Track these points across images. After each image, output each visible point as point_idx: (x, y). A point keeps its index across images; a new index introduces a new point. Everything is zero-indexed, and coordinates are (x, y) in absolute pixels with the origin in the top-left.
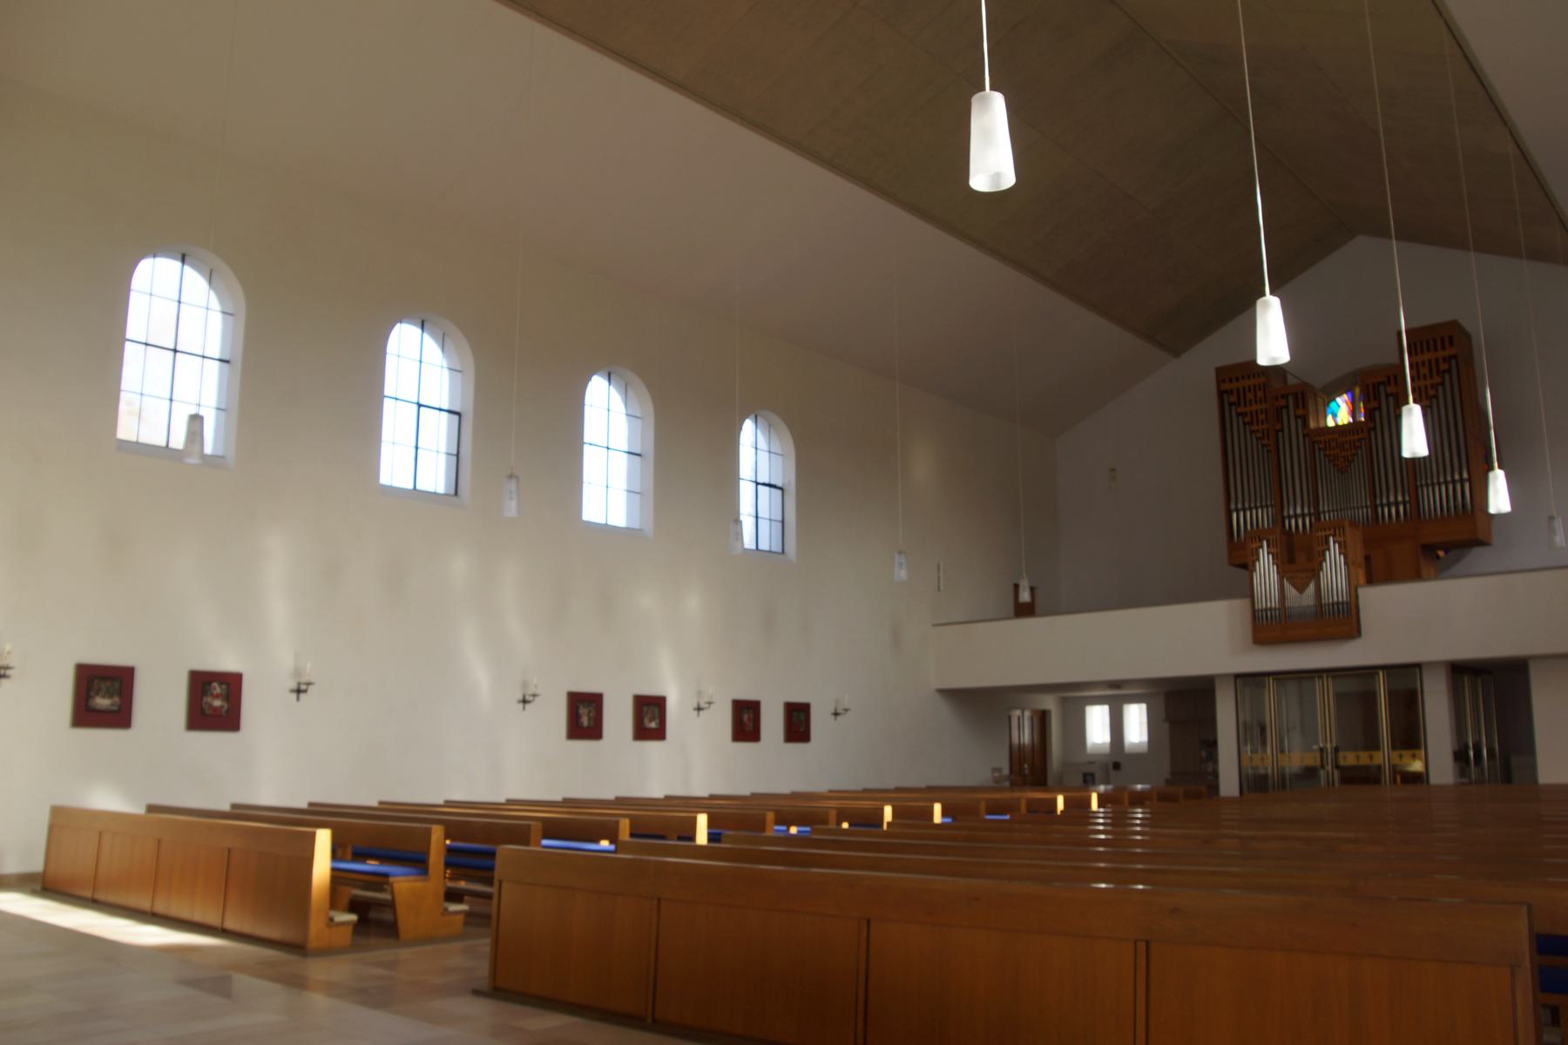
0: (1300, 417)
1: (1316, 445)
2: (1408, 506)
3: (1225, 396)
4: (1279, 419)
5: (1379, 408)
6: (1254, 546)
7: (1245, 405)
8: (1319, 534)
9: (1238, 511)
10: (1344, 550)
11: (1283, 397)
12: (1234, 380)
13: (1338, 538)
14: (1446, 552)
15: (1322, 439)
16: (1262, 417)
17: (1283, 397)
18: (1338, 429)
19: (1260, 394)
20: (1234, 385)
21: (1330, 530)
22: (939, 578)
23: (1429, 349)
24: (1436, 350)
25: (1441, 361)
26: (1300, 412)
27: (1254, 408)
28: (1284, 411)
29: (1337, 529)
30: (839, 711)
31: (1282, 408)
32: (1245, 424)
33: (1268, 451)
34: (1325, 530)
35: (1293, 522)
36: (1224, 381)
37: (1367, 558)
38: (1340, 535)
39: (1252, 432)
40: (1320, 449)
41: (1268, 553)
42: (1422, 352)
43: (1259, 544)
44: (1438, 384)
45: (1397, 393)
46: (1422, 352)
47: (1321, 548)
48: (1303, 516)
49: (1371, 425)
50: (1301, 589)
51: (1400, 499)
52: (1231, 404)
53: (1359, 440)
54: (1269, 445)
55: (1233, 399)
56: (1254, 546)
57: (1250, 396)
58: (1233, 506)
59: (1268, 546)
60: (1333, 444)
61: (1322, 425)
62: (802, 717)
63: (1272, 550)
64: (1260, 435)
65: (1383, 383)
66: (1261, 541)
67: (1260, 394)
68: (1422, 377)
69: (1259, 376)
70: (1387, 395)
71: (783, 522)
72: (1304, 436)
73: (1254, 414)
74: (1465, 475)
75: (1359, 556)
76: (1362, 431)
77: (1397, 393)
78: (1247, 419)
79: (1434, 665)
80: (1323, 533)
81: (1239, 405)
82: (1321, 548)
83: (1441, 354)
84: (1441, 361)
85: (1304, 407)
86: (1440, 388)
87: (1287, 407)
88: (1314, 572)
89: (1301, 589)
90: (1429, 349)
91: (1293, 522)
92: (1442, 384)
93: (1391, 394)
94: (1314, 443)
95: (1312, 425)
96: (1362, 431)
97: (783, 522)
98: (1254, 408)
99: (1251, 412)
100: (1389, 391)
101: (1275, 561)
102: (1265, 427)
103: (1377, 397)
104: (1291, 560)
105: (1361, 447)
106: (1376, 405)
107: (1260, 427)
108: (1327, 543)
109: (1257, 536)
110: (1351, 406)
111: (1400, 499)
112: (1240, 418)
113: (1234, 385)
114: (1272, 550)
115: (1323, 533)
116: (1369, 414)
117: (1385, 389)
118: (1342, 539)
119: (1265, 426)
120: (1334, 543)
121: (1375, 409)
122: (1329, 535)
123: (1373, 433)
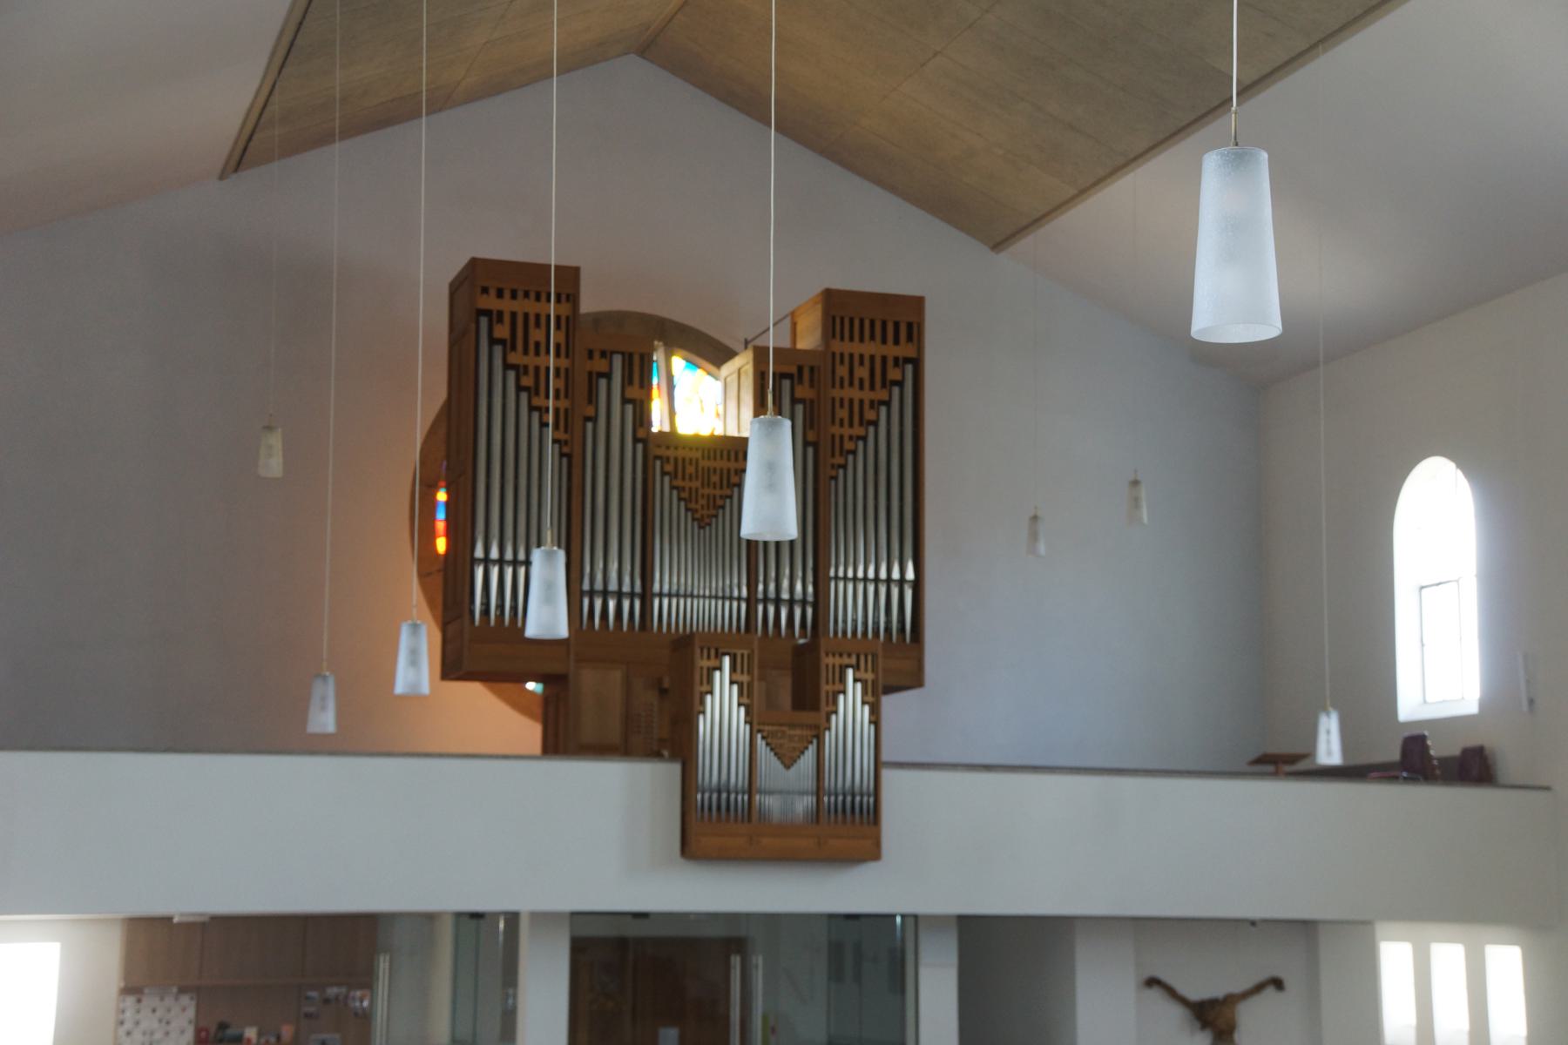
1: (658, 463)
2: (809, 611)
3: (484, 321)
4: (592, 397)
6: (705, 663)
7: (526, 352)
8: (830, 660)
9: (487, 561)
11: (603, 354)
12: (507, 294)
13: (862, 675)
15: (671, 453)
17: (603, 354)
20: (506, 305)
21: (849, 655)
23: (872, 337)
24: (884, 341)
25: (890, 363)
26: (634, 392)
28: (603, 382)
31: (601, 375)
34: (841, 655)
35: (598, 603)
36: (485, 290)
38: (866, 670)
40: (664, 473)
41: (732, 683)
42: (862, 340)
43: (713, 663)
45: (812, 401)
46: (862, 340)
47: (830, 688)
50: (788, 761)
52: (493, 341)
54: (566, 443)
56: (705, 663)
59: (733, 669)
63: (738, 677)
66: (719, 656)
68: (856, 382)
72: (636, 440)
74: (910, 575)
79: (937, 921)
80: (838, 661)
82: (830, 688)
83: (891, 351)
84: (890, 363)
85: (642, 386)
86: (883, 410)
87: (608, 376)
88: (818, 733)
89: (788, 761)
90: (872, 337)
91: (598, 603)
92: (888, 404)
94: (657, 457)
99: (537, 369)
100: (798, 395)
101: (745, 700)
108: (843, 680)
109: (717, 644)
111: (494, 554)
112: (511, 375)
113: (506, 305)
114: (738, 677)
120: (855, 680)
122: (848, 666)
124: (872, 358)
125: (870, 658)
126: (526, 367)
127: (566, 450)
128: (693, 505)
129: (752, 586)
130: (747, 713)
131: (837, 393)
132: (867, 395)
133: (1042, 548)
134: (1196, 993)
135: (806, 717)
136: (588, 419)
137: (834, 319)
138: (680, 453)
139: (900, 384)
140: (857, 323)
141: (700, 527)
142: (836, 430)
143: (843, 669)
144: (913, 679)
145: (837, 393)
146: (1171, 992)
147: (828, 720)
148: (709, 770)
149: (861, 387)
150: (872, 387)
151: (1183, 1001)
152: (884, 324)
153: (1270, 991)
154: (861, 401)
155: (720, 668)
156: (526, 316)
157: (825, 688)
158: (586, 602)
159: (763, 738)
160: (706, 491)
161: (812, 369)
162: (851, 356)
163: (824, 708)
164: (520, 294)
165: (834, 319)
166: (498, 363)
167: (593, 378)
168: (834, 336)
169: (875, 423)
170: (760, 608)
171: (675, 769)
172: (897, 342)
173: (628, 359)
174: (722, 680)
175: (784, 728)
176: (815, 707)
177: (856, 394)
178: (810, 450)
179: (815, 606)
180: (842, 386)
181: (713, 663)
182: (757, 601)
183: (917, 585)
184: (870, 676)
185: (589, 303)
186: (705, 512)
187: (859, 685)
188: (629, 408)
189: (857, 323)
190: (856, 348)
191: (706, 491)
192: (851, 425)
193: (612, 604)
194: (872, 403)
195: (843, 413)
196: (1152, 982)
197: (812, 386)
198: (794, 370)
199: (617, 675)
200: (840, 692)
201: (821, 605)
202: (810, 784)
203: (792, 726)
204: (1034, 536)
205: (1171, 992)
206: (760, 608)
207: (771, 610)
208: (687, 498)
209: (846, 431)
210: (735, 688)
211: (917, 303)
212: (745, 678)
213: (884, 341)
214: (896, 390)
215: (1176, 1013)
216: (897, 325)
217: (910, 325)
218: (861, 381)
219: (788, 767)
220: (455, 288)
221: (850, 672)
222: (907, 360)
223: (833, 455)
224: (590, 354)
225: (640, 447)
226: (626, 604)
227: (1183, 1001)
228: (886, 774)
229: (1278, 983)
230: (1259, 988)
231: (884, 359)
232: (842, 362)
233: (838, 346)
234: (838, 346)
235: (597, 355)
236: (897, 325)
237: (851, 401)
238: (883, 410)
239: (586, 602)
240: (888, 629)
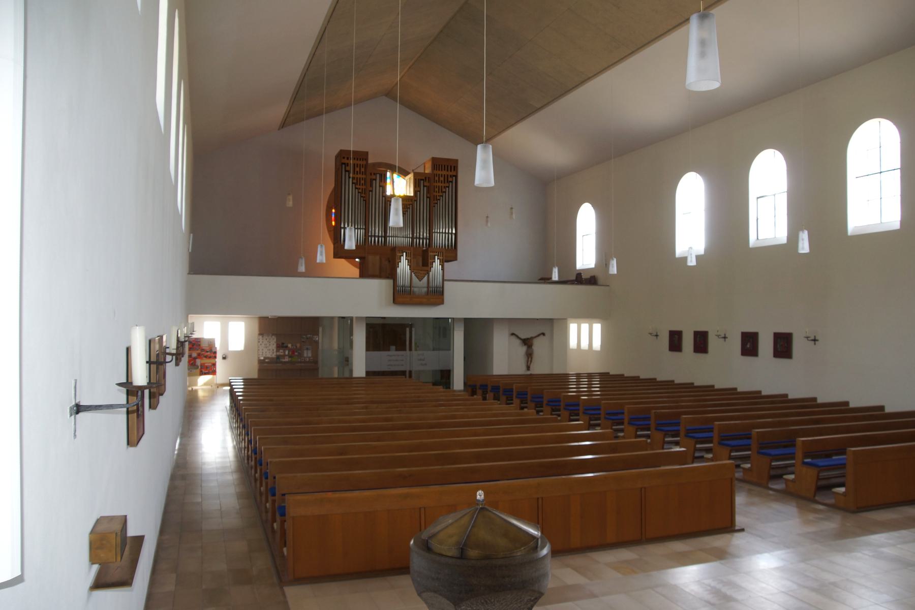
2: (428, 241)
3: (344, 166)
4: (371, 186)
5: (420, 191)
8: (431, 254)
11: (374, 174)
16: (362, 182)
17: (374, 174)
23: (445, 170)
24: (448, 171)
28: (374, 181)
31: (374, 179)
33: (363, 200)
35: (373, 239)
36: (344, 158)
41: (406, 259)
43: (401, 254)
44: (447, 187)
46: (442, 170)
47: (431, 261)
49: (416, 199)
50: (420, 279)
53: (409, 205)
54: (365, 197)
65: (423, 180)
66: (403, 252)
67: (363, 170)
69: (363, 160)
70: (424, 186)
72: (383, 196)
73: (359, 179)
74: (454, 232)
79: (459, 319)
80: (433, 254)
83: (450, 173)
86: (447, 189)
87: (376, 180)
88: (428, 272)
89: (420, 279)
90: (445, 170)
91: (373, 239)
92: (449, 187)
93: (426, 186)
99: (357, 178)
100: (425, 184)
102: (364, 187)
103: (419, 186)
106: (419, 190)
107: (361, 187)
108: (434, 259)
109: (402, 249)
115: (433, 254)
116: (415, 192)
117: (423, 183)
119: (364, 187)
121: (418, 191)
124: (444, 175)
127: (364, 199)
129: (413, 234)
130: (410, 267)
131: (435, 184)
132: (443, 185)
133: (489, 224)
134: (523, 337)
135: (425, 268)
136: (370, 191)
139: (452, 182)
142: (435, 194)
143: (435, 256)
144: (455, 258)
145: (435, 184)
146: (517, 337)
147: (431, 269)
148: (400, 282)
151: (520, 339)
152: (448, 166)
153: (542, 336)
154: (442, 186)
157: (430, 261)
158: (370, 238)
161: (429, 178)
163: (429, 266)
167: (371, 180)
168: (435, 169)
169: (445, 192)
170: (415, 240)
171: (391, 282)
172: (451, 171)
173: (381, 175)
174: (403, 259)
176: (427, 266)
177: (440, 184)
178: (428, 199)
179: (429, 239)
180: (436, 182)
181: (401, 254)
182: (414, 238)
183: (456, 234)
184: (441, 258)
185: (371, 161)
187: (439, 260)
188: (381, 188)
190: (440, 173)
192: (439, 192)
193: (377, 239)
194: (444, 187)
195: (437, 190)
196: (513, 334)
197: (429, 182)
198: (424, 178)
199: (378, 258)
201: (431, 239)
202: (426, 285)
203: (421, 270)
204: (487, 222)
205: (517, 337)
206: (415, 240)
207: (418, 240)
209: (438, 194)
210: (407, 261)
211: (457, 161)
212: (409, 258)
213: (448, 171)
214: (451, 184)
215: (518, 342)
216: (451, 167)
217: (454, 167)
218: (442, 181)
219: (420, 281)
220: (337, 157)
221: (436, 257)
222: (453, 176)
223: (434, 200)
224: (371, 174)
225: (384, 198)
226: (380, 239)
227: (520, 339)
228: (445, 282)
229: (544, 334)
230: (539, 335)
231: (448, 175)
233: (435, 172)
234: (435, 172)
236: (451, 167)
237: (439, 186)
238: (447, 189)
239: (370, 238)
240: (448, 246)
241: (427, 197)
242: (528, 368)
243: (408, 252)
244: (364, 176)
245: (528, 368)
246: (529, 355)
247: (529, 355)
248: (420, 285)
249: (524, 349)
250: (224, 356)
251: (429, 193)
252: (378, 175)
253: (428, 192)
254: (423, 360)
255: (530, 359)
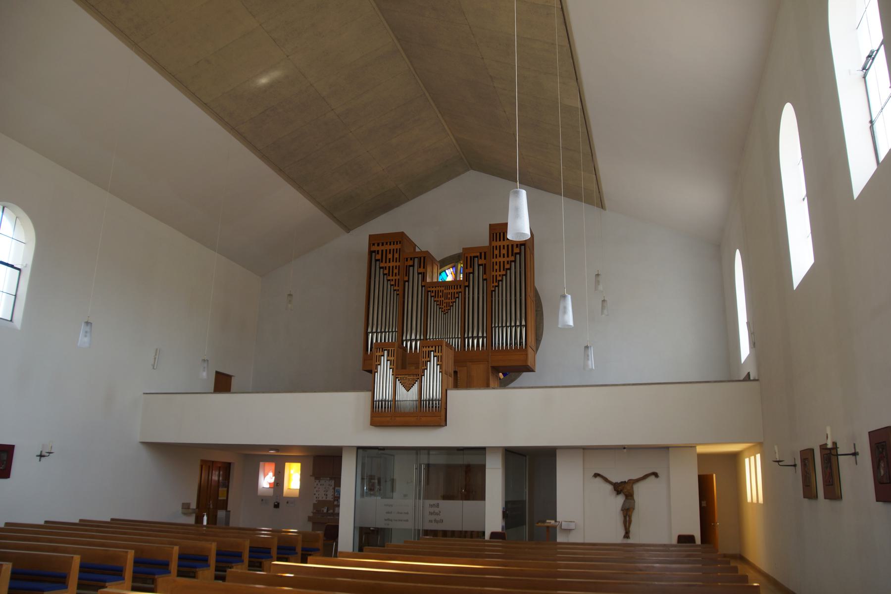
0: (421, 273)
1: (429, 293)
3: (374, 254)
4: (407, 274)
5: (473, 273)
6: (378, 354)
9: (372, 333)
10: (440, 359)
12: (381, 244)
13: (437, 354)
14: (504, 375)
15: (434, 289)
16: (396, 271)
17: (411, 259)
18: (445, 284)
19: (397, 256)
20: (380, 248)
22: (155, 358)
26: (421, 270)
27: (391, 264)
28: (411, 268)
29: (438, 346)
30: (44, 453)
31: (410, 266)
32: (384, 274)
33: (397, 294)
34: (429, 347)
35: (409, 343)
36: (374, 244)
37: (456, 372)
39: (388, 280)
40: (431, 297)
41: (387, 360)
45: (485, 264)
47: (424, 360)
48: (416, 340)
49: (467, 284)
51: (480, 335)
52: (376, 260)
54: (398, 290)
55: (379, 257)
56: (378, 354)
57: (390, 256)
58: (369, 330)
59: (388, 355)
60: (440, 294)
61: (435, 280)
62: (4, 456)
63: (389, 358)
64: (393, 283)
65: (477, 257)
66: (383, 351)
67: (397, 256)
68: (502, 256)
69: (397, 244)
70: (479, 265)
71: (16, 296)
72: (422, 286)
74: (523, 323)
75: (450, 367)
76: (460, 288)
77: (485, 264)
78: (386, 272)
79: (494, 449)
80: (427, 349)
81: (382, 262)
82: (424, 360)
87: (413, 266)
88: (418, 376)
91: (409, 343)
92: (515, 261)
93: (482, 265)
95: (428, 280)
96: (460, 288)
97: (16, 296)
98: (391, 264)
101: (392, 367)
102: (397, 277)
103: (472, 266)
104: (404, 367)
105: (458, 297)
107: (394, 278)
108: (429, 356)
109: (381, 347)
110: (454, 276)
112: (382, 270)
113: (380, 248)
114: (389, 358)
116: (467, 276)
118: (440, 354)
119: (397, 277)
120: (434, 356)
123: (467, 288)
124: (508, 246)
125: (440, 347)
126: (386, 267)
127: (398, 293)
128: (441, 307)
131: (495, 260)
132: (506, 259)
134: (614, 481)
137: (493, 234)
138: (437, 289)
139: (520, 254)
140: (498, 234)
141: (444, 314)
142: (494, 273)
143: (429, 352)
145: (495, 260)
146: (606, 480)
149: (504, 257)
150: (508, 256)
153: (653, 477)
154: (504, 262)
155: (383, 356)
156: (386, 250)
158: (405, 343)
159: (399, 380)
160: (446, 301)
161: (485, 253)
162: (500, 246)
164: (385, 244)
165: (493, 234)
166: (378, 267)
168: (493, 240)
169: (510, 269)
171: (369, 394)
174: (384, 360)
175: (406, 376)
176: (417, 368)
177: (502, 259)
181: (381, 354)
186: (446, 308)
189: (498, 234)
191: (446, 301)
192: (500, 271)
193: (414, 343)
194: (508, 262)
195: (497, 267)
198: (478, 254)
200: (428, 361)
205: (606, 480)
207: (471, 341)
208: (440, 304)
209: (498, 273)
215: (609, 488)
229: (656, 475)
232: (496, 249)
233: (494, 244)
234: (494, 244)
235: (409, 259)
237: (500, 262)
239: (405, 343)
240: (521, 343)
241: (484, 280)
242: (627, 535)
243: (390, 349)
244: (398, 264)
245: (627, 535)
246: (627, 512)
247: (627, 512)
248: (407, 396)
249: (621, 499)
250: (276, 504)
251: (485, 274)
252: (416, 260)
253: (485, 273)
254: (438, 514)
255: (628, 519)
